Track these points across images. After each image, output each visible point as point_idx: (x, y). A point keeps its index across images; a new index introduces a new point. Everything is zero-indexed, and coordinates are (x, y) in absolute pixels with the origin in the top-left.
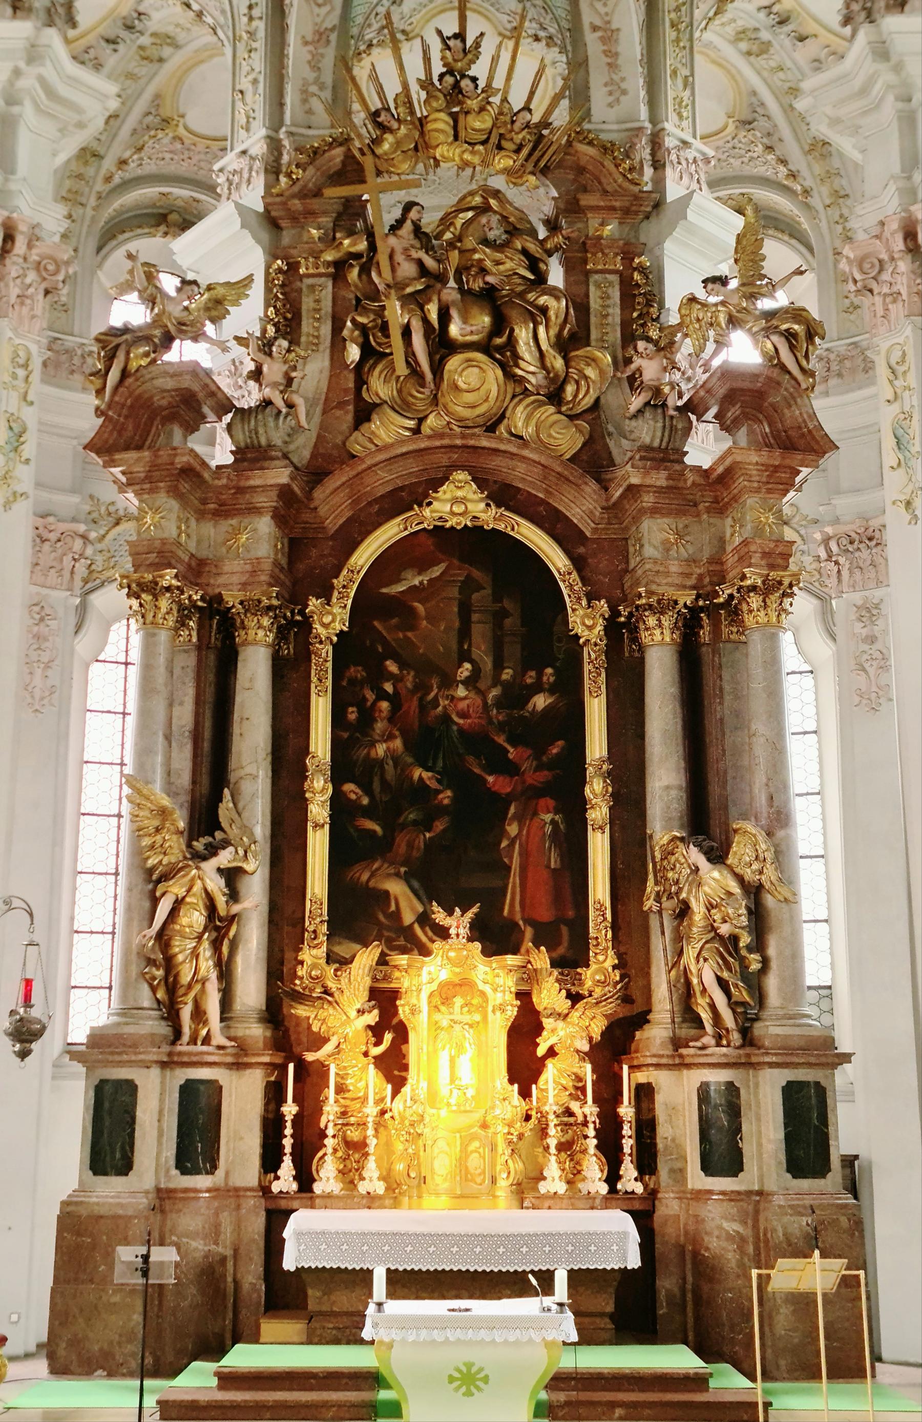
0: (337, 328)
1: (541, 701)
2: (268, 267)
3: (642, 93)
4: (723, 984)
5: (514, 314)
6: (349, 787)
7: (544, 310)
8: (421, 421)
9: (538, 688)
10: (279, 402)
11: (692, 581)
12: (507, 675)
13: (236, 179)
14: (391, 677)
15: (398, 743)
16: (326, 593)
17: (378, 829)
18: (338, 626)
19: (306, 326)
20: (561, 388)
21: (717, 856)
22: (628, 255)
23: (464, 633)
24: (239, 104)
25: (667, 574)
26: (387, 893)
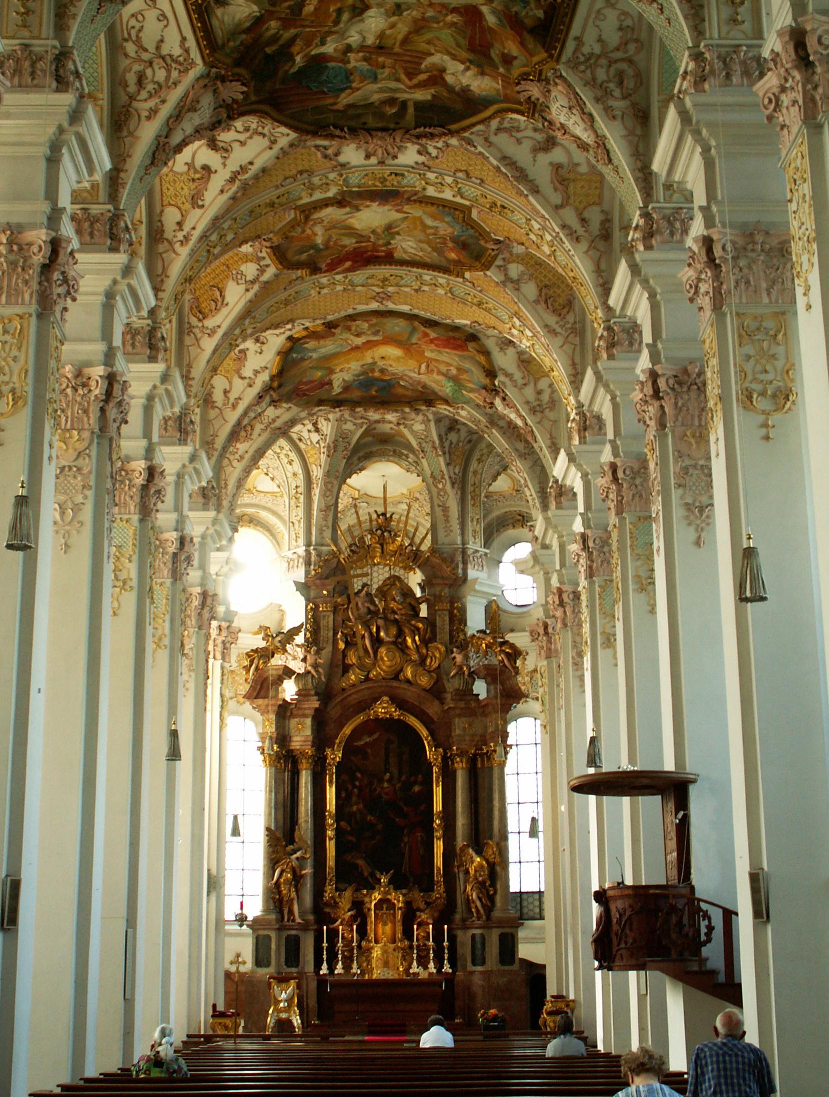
0: (335, 634)
1: (417, 788)
2: (306, 607)
3: (459, 531)
4: (480, 899)
5: (407, 631)
6: (343, 824)
7: (418, 629)
8: (369, 672)
9: (415, 783)
10: (313, 672)
11: (474, 743)
12: (404, 778)
13: (291, 563)
14: (357, 779)
15: (361, 806)
16: (332, 746)
17: (354, 840)
18: (338, 759)
19: (323, 633)
20: (425, 659)
21: (479, 852)
22: (452, 602)
23: (387, 762)
24: (292, 528)
25: (464, 740)
26: (357, 865)
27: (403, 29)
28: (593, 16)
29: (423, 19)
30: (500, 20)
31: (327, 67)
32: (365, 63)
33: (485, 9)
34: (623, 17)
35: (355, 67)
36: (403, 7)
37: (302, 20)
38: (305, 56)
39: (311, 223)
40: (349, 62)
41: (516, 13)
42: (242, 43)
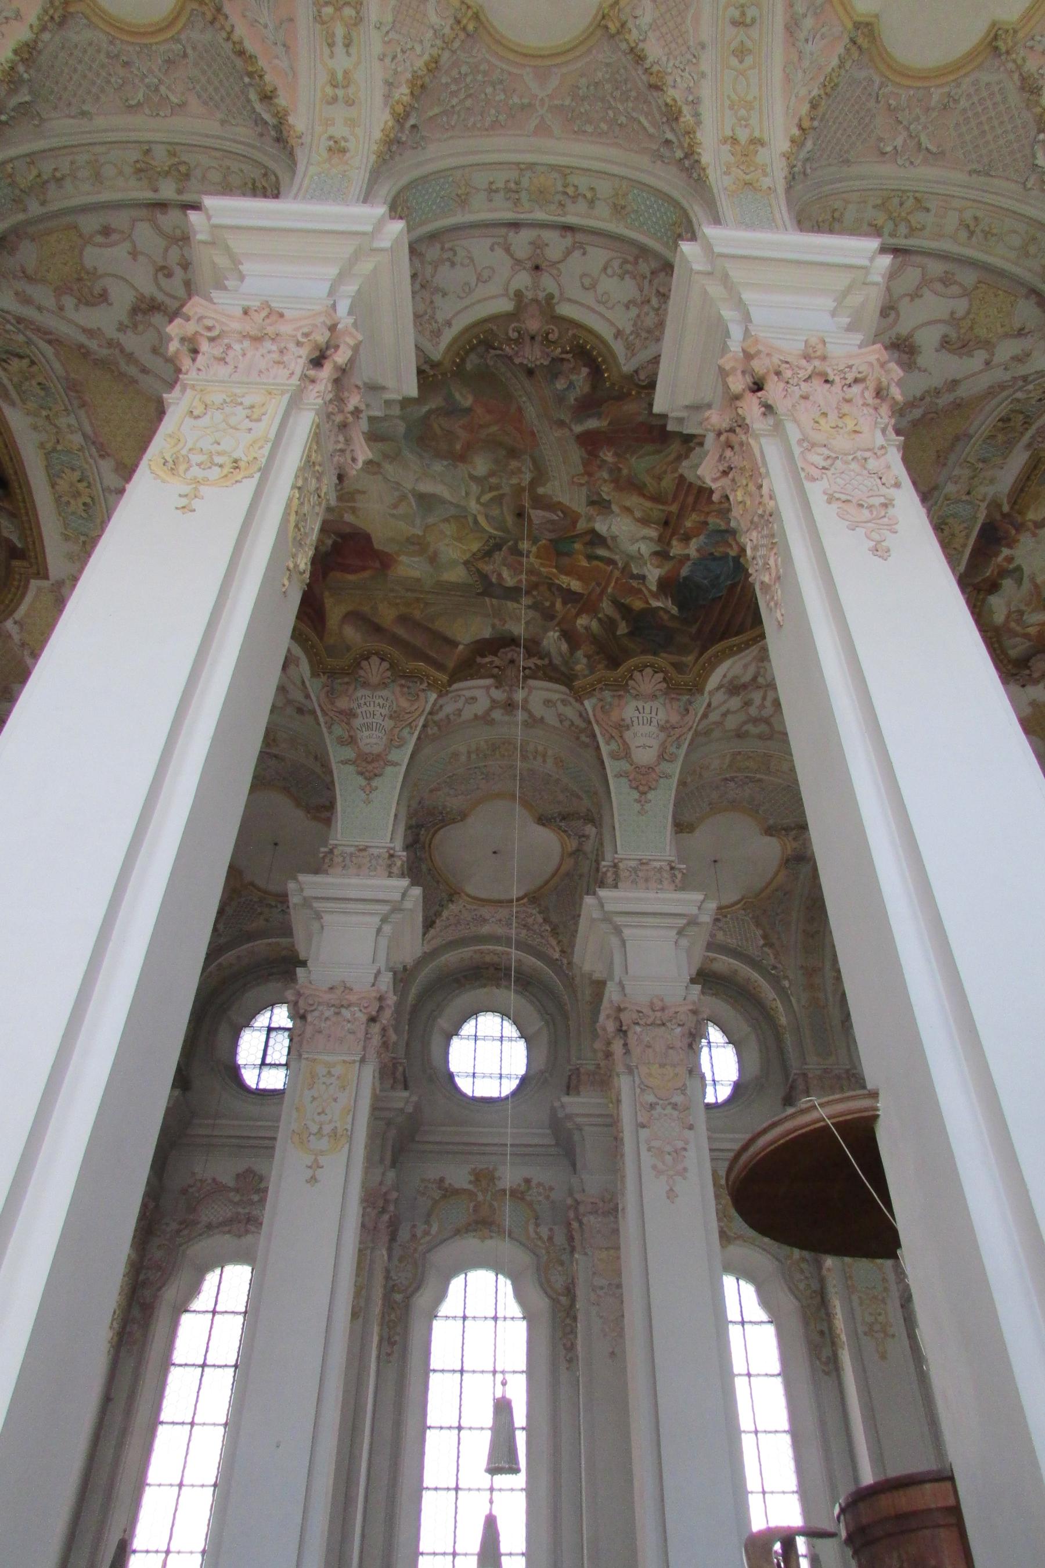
27: (634, 500)
28: (601, 309)
29: (616, 481)
30: (589, 416)
31: (685, 578)
32: (694, 540)
33: (578, 429)
34: (609, 271)
35: (698, 550)
36: (595, 498)
37: (590, 594)
38: (655, 596)
39: (1013, 625)
40: (687, 557)
41: (576, 400)
42: (588, 657)
